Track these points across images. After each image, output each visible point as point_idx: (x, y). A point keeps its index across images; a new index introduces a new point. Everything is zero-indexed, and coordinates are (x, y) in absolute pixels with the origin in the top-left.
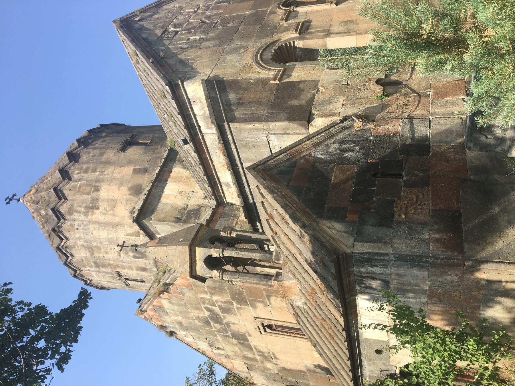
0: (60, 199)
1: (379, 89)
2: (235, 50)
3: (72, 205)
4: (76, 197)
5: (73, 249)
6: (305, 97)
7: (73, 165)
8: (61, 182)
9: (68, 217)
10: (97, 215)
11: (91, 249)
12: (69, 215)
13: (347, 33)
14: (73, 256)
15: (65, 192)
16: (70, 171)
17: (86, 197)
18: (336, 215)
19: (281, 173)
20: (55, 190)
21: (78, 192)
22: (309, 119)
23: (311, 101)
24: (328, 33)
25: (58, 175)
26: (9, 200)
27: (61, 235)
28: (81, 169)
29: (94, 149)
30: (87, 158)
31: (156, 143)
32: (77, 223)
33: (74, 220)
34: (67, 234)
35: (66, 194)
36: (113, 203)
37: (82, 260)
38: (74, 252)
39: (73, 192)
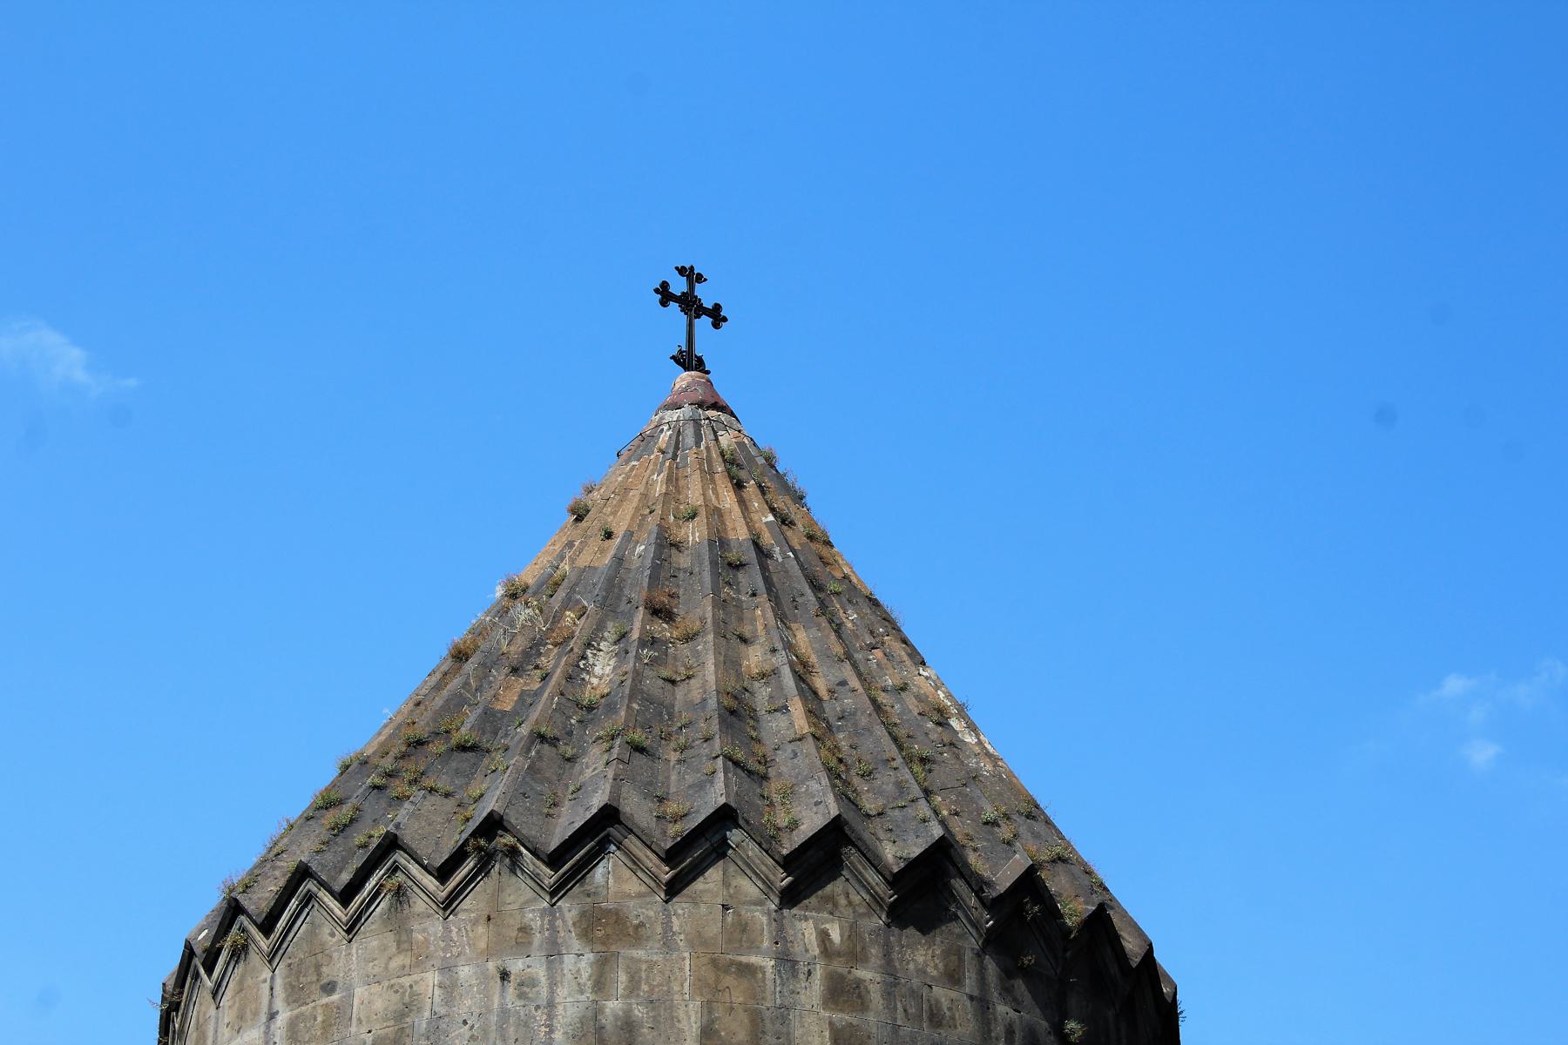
0: (670, 857)
3: (637, 935)
5: (390, 938)
7: (876, 898)
8: (767, 842)
9: (569, 908)
12: (583, 914)
14: (352, 928)
15: (714, 874)
16: (836, 888)
20: (725, 817)
21: (714, 963)
25: (810, 814)
26: (687, 300)
27: (470, 864)
28: (855, 955)
29: (982, 1004)
30: (922, 972)
32: (540, 972)
34: (472, 903)
35: (698, 885)
37: (329, 988)
38: (373, 935)
39: (713, 930)
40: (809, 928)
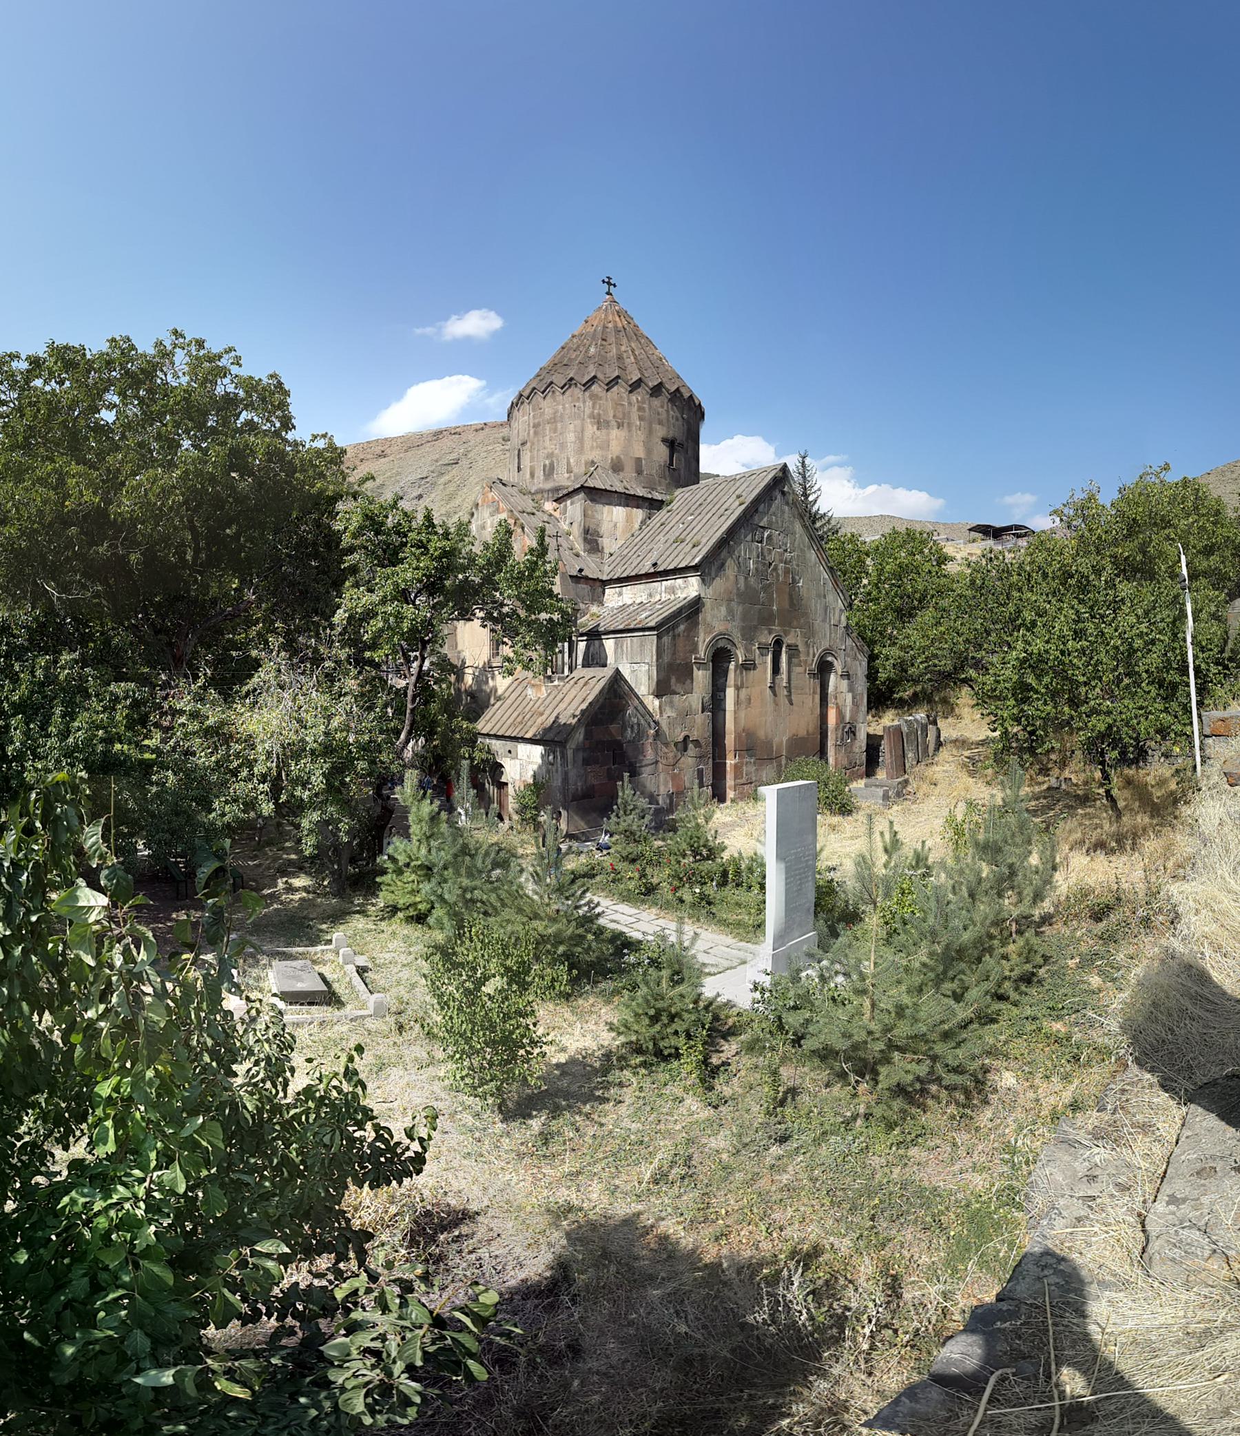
1: (681, 738)
2: (730, 611)
3: (601, 399)
4: (610, 401)
6: (678, 688)
9: (587, 394)
10: (591, 429)
11: (553, 420)
13: (737, 702)
17: (611, 414)
18: (588, 735)
19: (615, 691)
20: (618, 377)
22: (658, 695)
23: (675, 693)
24: (738, 688)
31: (672, 476)
33: (584, 402)
36: (605, 446)
40: (634, 397)
